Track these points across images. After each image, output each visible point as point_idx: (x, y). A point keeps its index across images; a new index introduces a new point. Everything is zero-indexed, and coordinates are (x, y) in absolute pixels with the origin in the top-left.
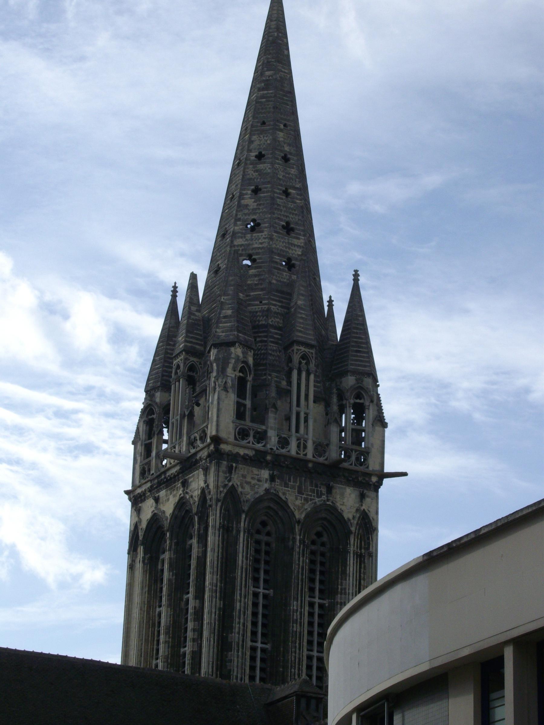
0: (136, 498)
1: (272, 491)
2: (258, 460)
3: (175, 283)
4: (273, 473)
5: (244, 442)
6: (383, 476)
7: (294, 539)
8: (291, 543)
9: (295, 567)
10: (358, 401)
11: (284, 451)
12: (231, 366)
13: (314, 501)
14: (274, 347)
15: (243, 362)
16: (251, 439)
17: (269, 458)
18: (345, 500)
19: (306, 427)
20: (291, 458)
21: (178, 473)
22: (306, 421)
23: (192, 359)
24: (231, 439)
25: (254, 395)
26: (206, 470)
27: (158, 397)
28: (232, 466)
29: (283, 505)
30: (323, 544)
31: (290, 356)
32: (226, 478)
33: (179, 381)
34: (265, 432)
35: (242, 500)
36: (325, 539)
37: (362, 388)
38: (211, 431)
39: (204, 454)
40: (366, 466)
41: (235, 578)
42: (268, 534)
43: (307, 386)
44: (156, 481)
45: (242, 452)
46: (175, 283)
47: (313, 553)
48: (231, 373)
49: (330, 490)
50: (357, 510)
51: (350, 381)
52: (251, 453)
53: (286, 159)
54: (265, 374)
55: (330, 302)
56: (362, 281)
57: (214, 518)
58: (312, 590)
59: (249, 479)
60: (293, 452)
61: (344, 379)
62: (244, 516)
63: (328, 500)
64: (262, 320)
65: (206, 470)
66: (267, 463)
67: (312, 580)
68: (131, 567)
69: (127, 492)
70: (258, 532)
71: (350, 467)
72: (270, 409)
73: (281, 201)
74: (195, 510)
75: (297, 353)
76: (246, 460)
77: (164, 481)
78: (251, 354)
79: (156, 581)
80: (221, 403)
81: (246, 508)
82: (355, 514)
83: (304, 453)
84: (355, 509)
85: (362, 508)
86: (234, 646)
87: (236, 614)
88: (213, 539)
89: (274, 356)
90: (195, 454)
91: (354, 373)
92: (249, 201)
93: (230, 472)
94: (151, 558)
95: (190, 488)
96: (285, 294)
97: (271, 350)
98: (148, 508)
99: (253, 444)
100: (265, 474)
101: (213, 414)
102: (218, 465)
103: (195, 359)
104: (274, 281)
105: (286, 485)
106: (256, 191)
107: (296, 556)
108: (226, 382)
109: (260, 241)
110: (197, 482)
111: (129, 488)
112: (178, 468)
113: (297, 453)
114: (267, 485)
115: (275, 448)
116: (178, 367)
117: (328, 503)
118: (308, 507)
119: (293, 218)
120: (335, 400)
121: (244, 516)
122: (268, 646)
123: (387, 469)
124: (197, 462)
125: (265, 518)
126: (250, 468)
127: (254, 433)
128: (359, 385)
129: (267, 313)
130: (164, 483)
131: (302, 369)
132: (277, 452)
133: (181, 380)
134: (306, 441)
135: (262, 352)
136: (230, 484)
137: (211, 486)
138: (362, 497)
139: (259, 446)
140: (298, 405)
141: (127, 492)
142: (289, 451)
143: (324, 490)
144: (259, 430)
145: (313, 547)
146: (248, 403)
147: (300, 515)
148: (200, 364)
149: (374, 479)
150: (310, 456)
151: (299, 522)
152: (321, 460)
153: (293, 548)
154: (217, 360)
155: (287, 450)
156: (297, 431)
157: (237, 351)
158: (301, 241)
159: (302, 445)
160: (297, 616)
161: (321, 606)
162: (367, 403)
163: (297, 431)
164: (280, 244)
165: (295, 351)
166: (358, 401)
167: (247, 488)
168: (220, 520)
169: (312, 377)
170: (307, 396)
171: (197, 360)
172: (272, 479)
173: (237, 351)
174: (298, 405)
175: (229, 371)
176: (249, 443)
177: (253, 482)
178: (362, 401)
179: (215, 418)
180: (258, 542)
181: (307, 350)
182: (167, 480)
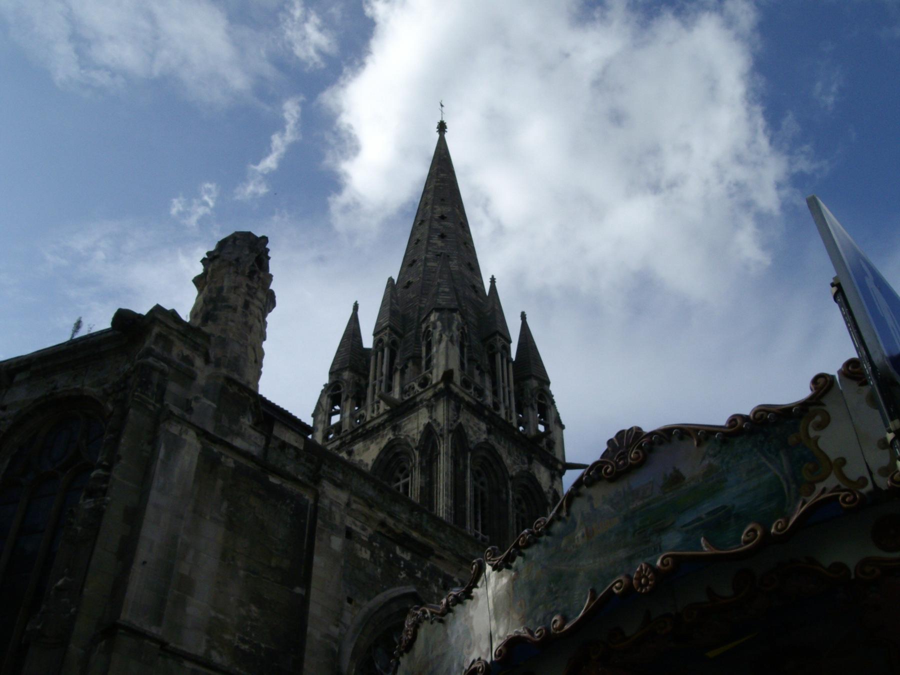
2: (478, 410)
5: (468, 391)
8: (504, 496)
21: (386, 421)
26: (431, 408)
29: (499, 460)
33: (383, 351)
41: (465, 509)
45: (467, 398)
49: (530, 461)
50: (551, 487)
51: (534, 383)
60: (503, 416)
62: (469, 455)
65: (431, 408)
77: (365, 433)
81: (472, 446)
88: (444, 466)
100: (483, 426)
102: (448, 401)
105: (499, 443)
107: (511, 509)
112: (385, 417)
121: (469, 455)
123: (568, 460)
124: (415, 404)
138: (553, 478)
139: (480, 400)
143: (526, 461)
151: (512, 478)
153: (507, 501)
157: (457, 316)
172: (489, 432)
173: (457, 316)
175: (454, 328)
177: (475, 429)
182: (368, 431)
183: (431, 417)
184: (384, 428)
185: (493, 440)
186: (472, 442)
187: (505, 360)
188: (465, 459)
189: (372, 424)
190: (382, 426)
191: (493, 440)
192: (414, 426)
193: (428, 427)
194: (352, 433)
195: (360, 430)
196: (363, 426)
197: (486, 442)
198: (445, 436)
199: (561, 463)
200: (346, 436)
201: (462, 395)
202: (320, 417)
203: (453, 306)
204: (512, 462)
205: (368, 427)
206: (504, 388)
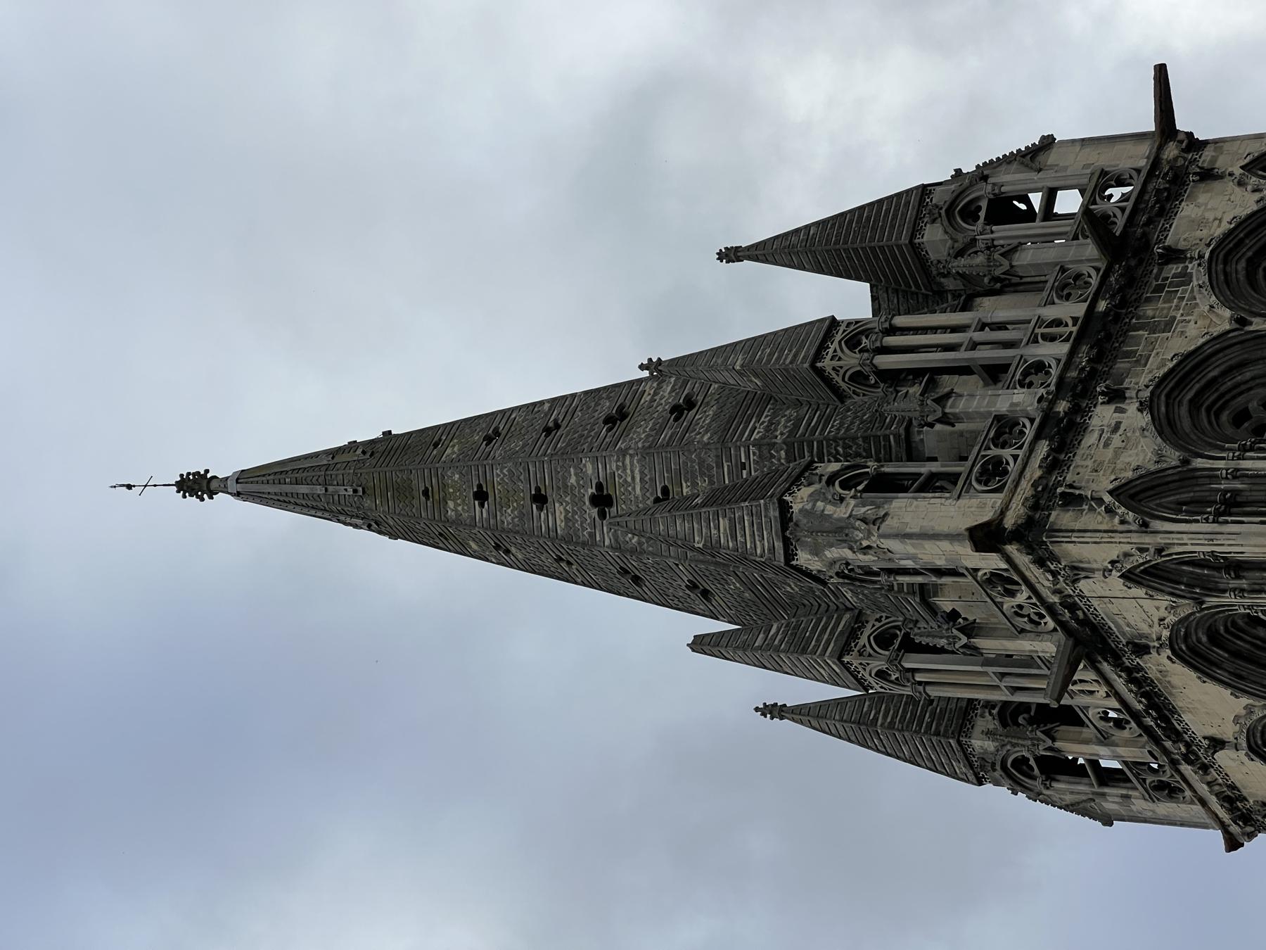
1: (1147, 394)
2: (1063, 433)
3: (757, 709)
4: (1102, 393)
10: (982, 214)
11: (1054, 372)
12: (830, 509)
13: (1196, 289)
16: (1006, 453)
18: (1210, 216)
21: (1117, 662)
22: (1001, 326)
23: (863, 640)
24: (997, 500)
26: (1077, 572)
27: (980, 744)
28: (1063, 494)
29: (1190, 365)
31: (851, 378)
32: (1092, 509)
35: (1153, 468)
40: (1134, 174)
44: (1168, 744)
45: (1034, 471)
46: (757, 709)
48: (849, 508)
49: (1174, 255)
50: (1241, 184)
51: (934, 237)
52: (1043, 448)
54: (887, 438)
56: (746, 240)
57: (1190, 537)
59: (1109, 453)
60: (1062, 349)
61: (933, 256)
62: (1199, 463)
63: (1201, 257)
64: (779, 460)
66: (1076, 410)
69: (1233, 844)
71: (1127, 212)
72: (947, 410)
75: (840, 359)
77: (1157, 716)
80: (908, 530)
81: (1173, 457)
82: (1249, 188)
83: (1070, 323)
84: (1237, 189)
85: (1238, 171)
89: (852, 423)
91: (916, 230)
92: (558, 514)
93: (1080, 499)
95: (1145, 629)
97: (838, 429)
99: (1020, 448)
100: (1103, 415)
101: (936, 553)
104: (705, 439)
106: (540, 499)
108: (864, 520)
109: (629, 479)
111: (1216, 837)
112: (1106, 667)
113: (1067, 340)
114: (1132, 408)
115: (1042, 391)
116: (882, 675)
117: (1207, 256)
118: (1206, 300)
121: (1199, 463)
123: (1148, 123)
126: (1080, 452)
127: (996, 446)
128: (943, 212)
129: (765, 445)
130: (1168, 721)
131: (878, 344)
132: (1052, 388)
133: (907, 665)
134: (1040, 322)
135: (840, 449)
136: (1108, 498)
137: (1114, 552)
138: (1208, 175)
139: (1030, 432)
141: (1233, 844)
142: (1059, 361)
143: (1174, 269)
144: (992, 434)
147: (1223, 320)
148: (879, 620)
150: (1080, 310)
151: (1242, 322)
152: (1094, 281)
154: (816, 551)
155: (1053, 364)
157: (800, 499)
159: (1049, 331)
164: (640, 433)
165: (835, 363)
166: (982, 214)
168: (1197, 521)
169: (900, 321)
171: (869, 626)
172: (1116, 396)
173: (800, 499)
176: (1015, 457)
178: (984, 204)
179: (945, 545)
181: (838, 337)
182: (1151, 705)
183: (1106, 572)
184: (1139, 668)
185: (1141, 380)
186: (1160, 457)
187: (891, 340)
188: (1212, 475)
189: (1130, 698)
191: (1141, 380)
192: (1139, 613)
193: (1130, 577)
194: (1157, 741)
195: (1149, 721)
196: (1136, 716)
197: (1147, 406)
198: (1160, 540)
199: (1161, 148)
200: (1166, 752)
201: (1025, 489)
202: (1110, 805)
203: (774, 513)
204: (1193, 319)
205: (1140, 707)
206: (974, 346)
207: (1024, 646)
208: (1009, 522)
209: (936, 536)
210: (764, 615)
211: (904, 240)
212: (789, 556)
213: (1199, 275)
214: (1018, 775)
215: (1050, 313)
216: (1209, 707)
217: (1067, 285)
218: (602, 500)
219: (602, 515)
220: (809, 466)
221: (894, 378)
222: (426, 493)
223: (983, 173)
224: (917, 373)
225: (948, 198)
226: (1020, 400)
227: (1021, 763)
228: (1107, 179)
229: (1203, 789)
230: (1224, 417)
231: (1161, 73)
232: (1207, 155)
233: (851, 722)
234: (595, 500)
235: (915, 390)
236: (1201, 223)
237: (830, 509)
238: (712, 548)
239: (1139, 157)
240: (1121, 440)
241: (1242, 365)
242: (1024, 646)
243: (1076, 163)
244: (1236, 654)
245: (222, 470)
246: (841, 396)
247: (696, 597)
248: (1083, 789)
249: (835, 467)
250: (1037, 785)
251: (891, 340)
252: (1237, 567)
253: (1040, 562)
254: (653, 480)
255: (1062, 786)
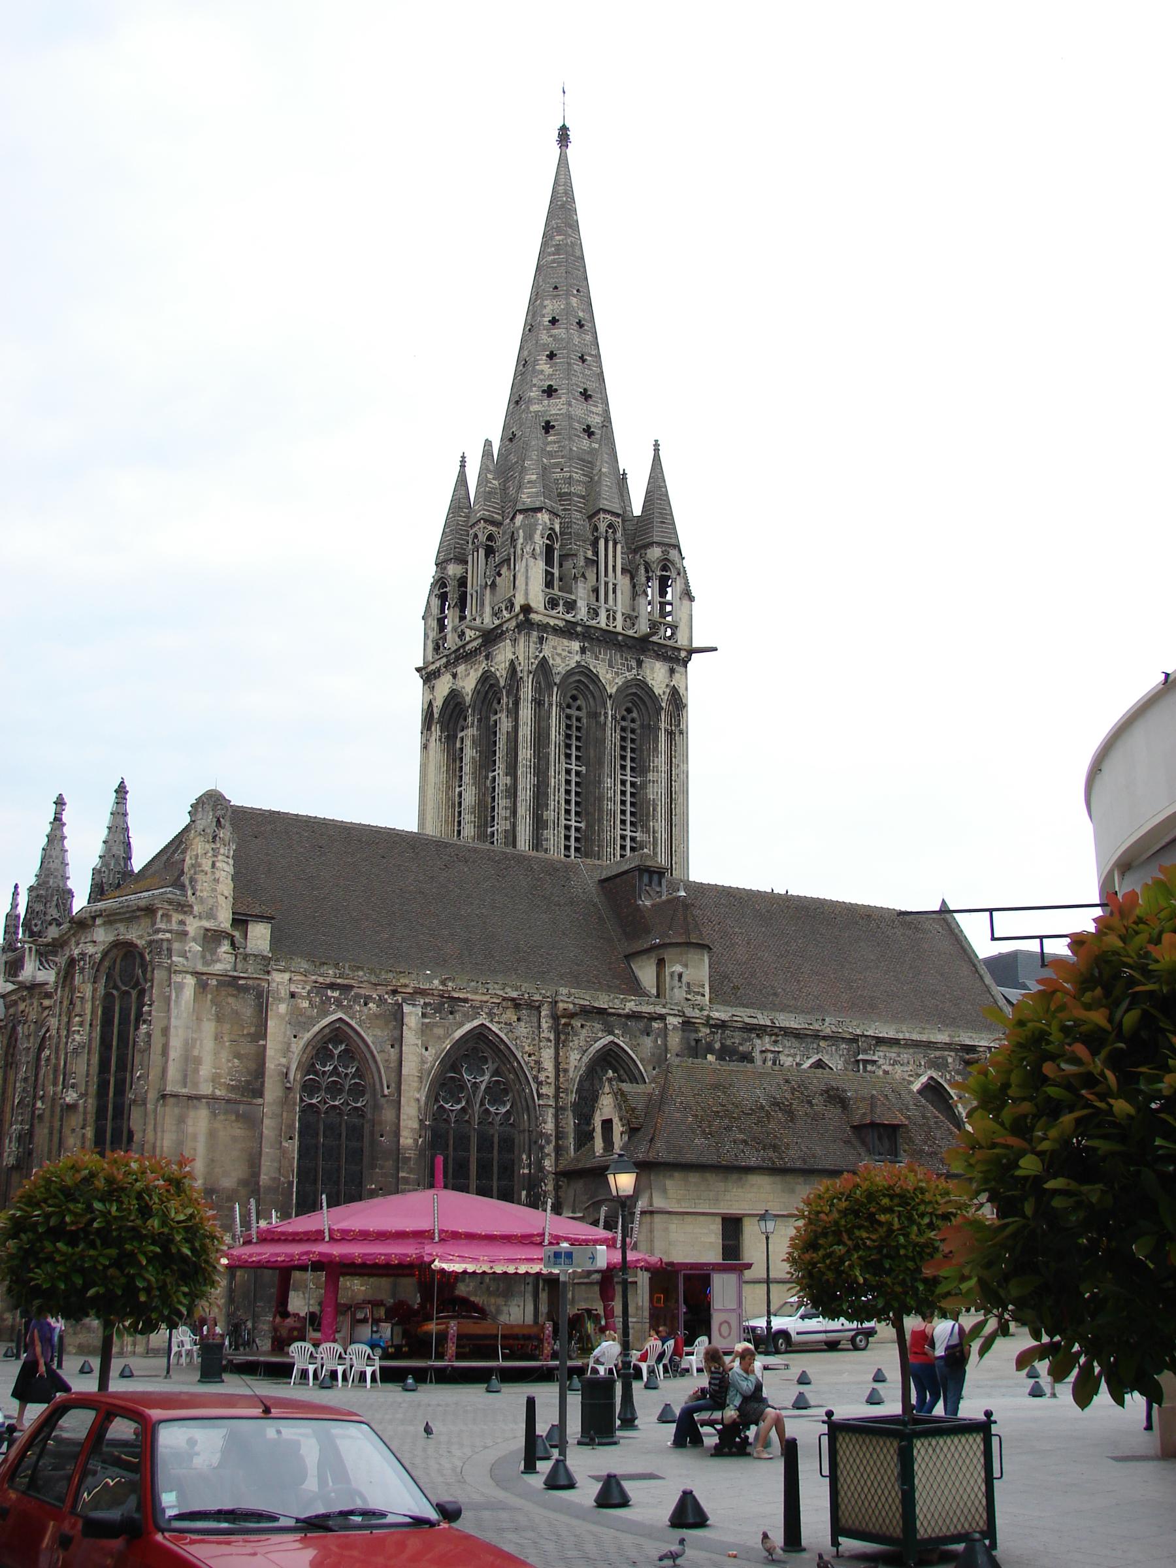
0: (429, 676)
2: (568, 631)
6: (692, 651)
7: (606, 713)
9: (608, 744)
11: (593, 623)
12: (538, 532)
14: (579, 516)
15: (551, 529)
16: (561, 608)
17: (579, 629)
19: (615, 600)
20: (601, 629)
22: (614, 592)
23: (490, 528)
24: (541, 609)
25: (561, 566)
27: (453, 570)
29: (594, 678)
30: (633, 721)
34: (575, 601)
36: (635, 715)
37: (668, 560)
38: (519, 601)
39: (514, 623)
42: (579, 709)
43: (615, 557)
45: (552, 622)
47: (623, 729)
48: (539, 541)
49: (640, 663)
51: (655, 553)
52: (561, 624)
53: (580, 325)
55: (624, 474)
57: (527, 692)
58: (623, 767)
59: (559, 651)
60: (603, 625)
61: (648, 551)
62: (555, 689)
66: (578, 635)
67: (623, 758)
68: (425, 747)
69: (418, 670)
70: (569, 706)
73: (578, 367)
74: (502, 683)
76: (556, 631)
77: (463, 656)
78: (557, 521)
79: (454, 761)
81: (557, 681)
86: (551, 824)
87: (551, 790)
88: (526, 713)
90: (501, 625)
91: (659, 544)
92: (544, 366)
94: (448, 737)
96: (588, 463)
98: (444, 686)
100: (576, 645)
103: (494, 529)
105: (597, 658)
106: (551, 356)
110: (504, 654)
111: (421, 665)
112: (480, 641)
114: (578, 658)
116: (476, 536)
118: (620, 681)
119: (591, 386)
120: (642, 570)
121: (555, 689)
122: (582, 825)
124: (503, 633)
125: (575, 692)
139: (569, 617)
140: (606, 575)
141: (418, 670)
143: (634, 664)
145: (623, 723)
146: (556, 571)
147: (612, 690)
149: (683, 654)
150: (619, 629)
151: (610, 697)
152: (630, 633)
154: (523, 526)
156: (606, 602)
157: (543, 517)
158: (599, 410)
160: (610, 794)
161: (633, 784)
162: (674, 575)
163: (606, 602)
164: (579, 409)
167: (558, 660)
169: (619, 547)
170: (614, 567)
172: (583, 650)
174: (606, 575)
175: (537, 537)
177: (565, 654)
179: (524, 587)
180: (569, 717)
187: (611, 544)
190: (476, 652)
196: (463, 646)
201: (546, 620)
202: (430, 620)
203: (538, 505)
204: (611, 675)
207: (488, 610)
208: (532, 616)
209: (527, 584)
210: (504, 466)
211: (656, 539)
212: (521, 511)
213: (629, 675)
214: (440, 583)
215: (619, 616)
216: (468, 681)
217: (631, 619)
218: (550, 392)
219: (544, 391)
220: (557, 515)
221: (595, 544)
222: (556, 288)
223: (681, 572)
224: (596, 553)
225: (671, 558)
226: (582, 613)
227: (444, 585)
228: (674, 628)
229: (437, 665)
230: (575, 692)
231: (715, 649)
232: (682, 669)
233: (459, 503)
234: (550, 386)
235: (590, 554)
236: (652, 669)
237: (538, 532)
238: (523, 470)
239: (682, 641)
240: (565, 655)
241: (594, 697)
242: (488, 610)
243: (682, 615)
244: (487, 692)
245: (570, 151)
246: (590, 517)
247: (509, 437)
248: (435, 610)
249: (557, 530)
250: (437, 592)
251: (611, 544)
252: (516, 703)
253: (517, 626)
254: (556, 420)
255: (436, 602)
